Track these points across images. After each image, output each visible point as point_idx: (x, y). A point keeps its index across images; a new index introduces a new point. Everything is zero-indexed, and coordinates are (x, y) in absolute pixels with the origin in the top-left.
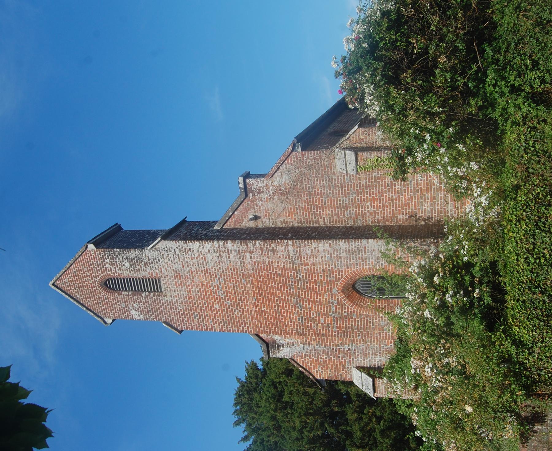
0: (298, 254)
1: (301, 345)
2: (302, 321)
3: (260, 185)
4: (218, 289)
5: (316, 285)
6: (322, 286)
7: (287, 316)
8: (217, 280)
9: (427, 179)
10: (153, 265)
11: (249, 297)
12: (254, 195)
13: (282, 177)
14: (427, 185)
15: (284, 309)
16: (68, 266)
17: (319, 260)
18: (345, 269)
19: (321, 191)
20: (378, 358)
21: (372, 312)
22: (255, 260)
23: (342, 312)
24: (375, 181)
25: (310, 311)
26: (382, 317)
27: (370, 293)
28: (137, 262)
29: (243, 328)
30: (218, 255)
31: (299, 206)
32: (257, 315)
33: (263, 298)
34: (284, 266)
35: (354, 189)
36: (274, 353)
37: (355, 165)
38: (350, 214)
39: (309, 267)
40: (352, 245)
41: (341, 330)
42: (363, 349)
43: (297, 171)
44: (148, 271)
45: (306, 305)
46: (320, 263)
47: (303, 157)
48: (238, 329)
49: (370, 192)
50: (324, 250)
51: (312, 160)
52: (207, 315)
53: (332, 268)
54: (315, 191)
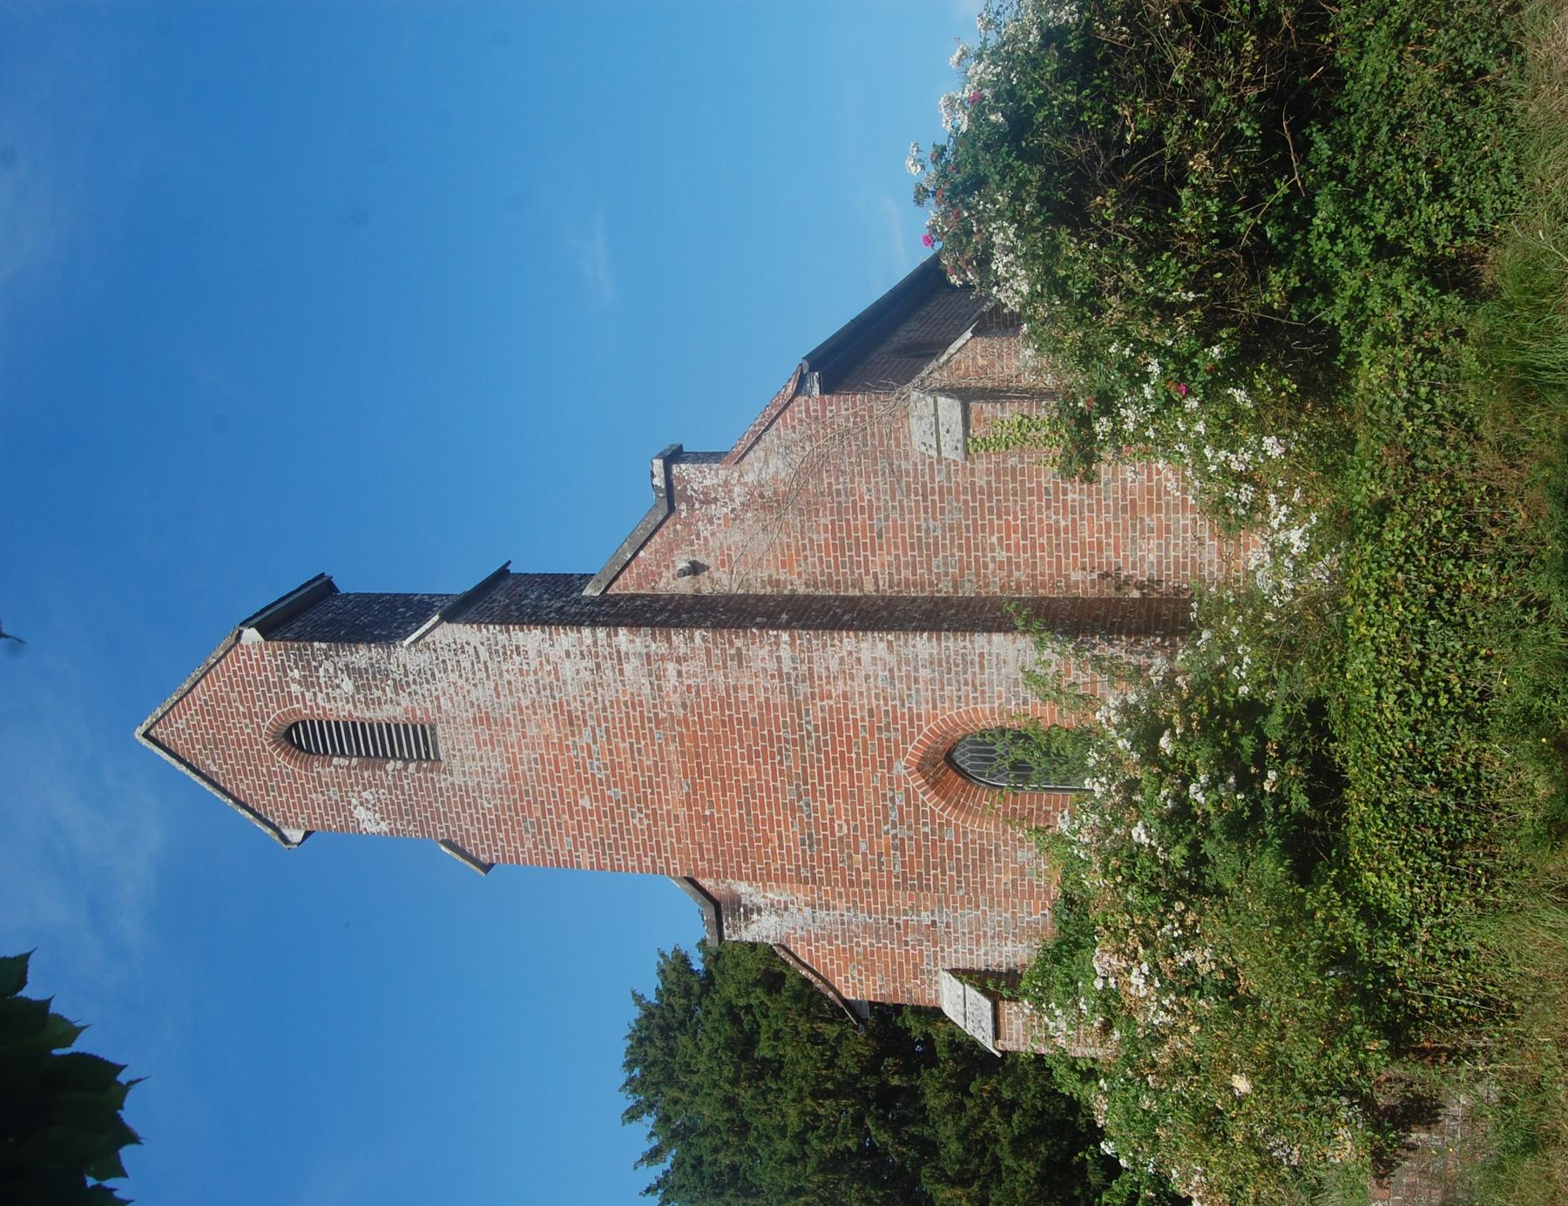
0: (805, 667)
1: (807, 911)
2: (811, 846)
3: (707, 482)
4: (590, 757)
5: (850, 752)
6: (865, 753)
7: (772, 831)
8: (587, 732)
9: (1150, 479)
10: (418, 688)
11: (672, 778)
12: (691, 508)
13: (766, 462)
14: (1150, 492)
15: (763, 813)
16: (186, 687)
17: (858, 685)
18: (928, 712)
19: (870, 501)
20: (1009, 948)
21: (996, 825)
22: (690, 682)
23: (917, 822)
24: (1014, 480)
25: (832, 820)
26: (1020, 840)
27: (991, 775)
28: (374, 679)
29: (653, 862)
30: (591, 664)
31: (811, 540)
32: (692, 828)
33: (708, 782)
34: (767, 699)
35: (958, 500)
36: (736, 929)
37: (960, 437)
38: (946, 564)
39: (832, 702)
40: (947, 648)
41: (912, 872)
42: (970, 924)
43: (808, 448)
44: (404, 704)
45: (823, 803)
46: (861, 693)
47: (824, 412)
48: (640, 863)
49: (999, 509)
50: (874, 659)
51: (848, 420)
52: (559, 825)
53: (894, 707)
54: (854, 502)
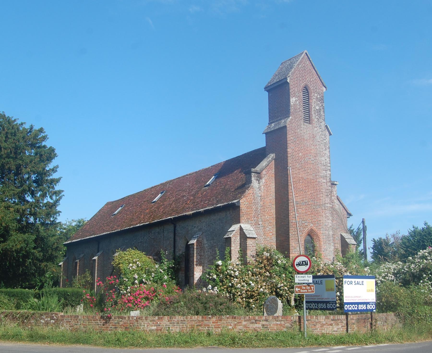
8: (313, 159)
30: (325, 164)
36: (254, 176)
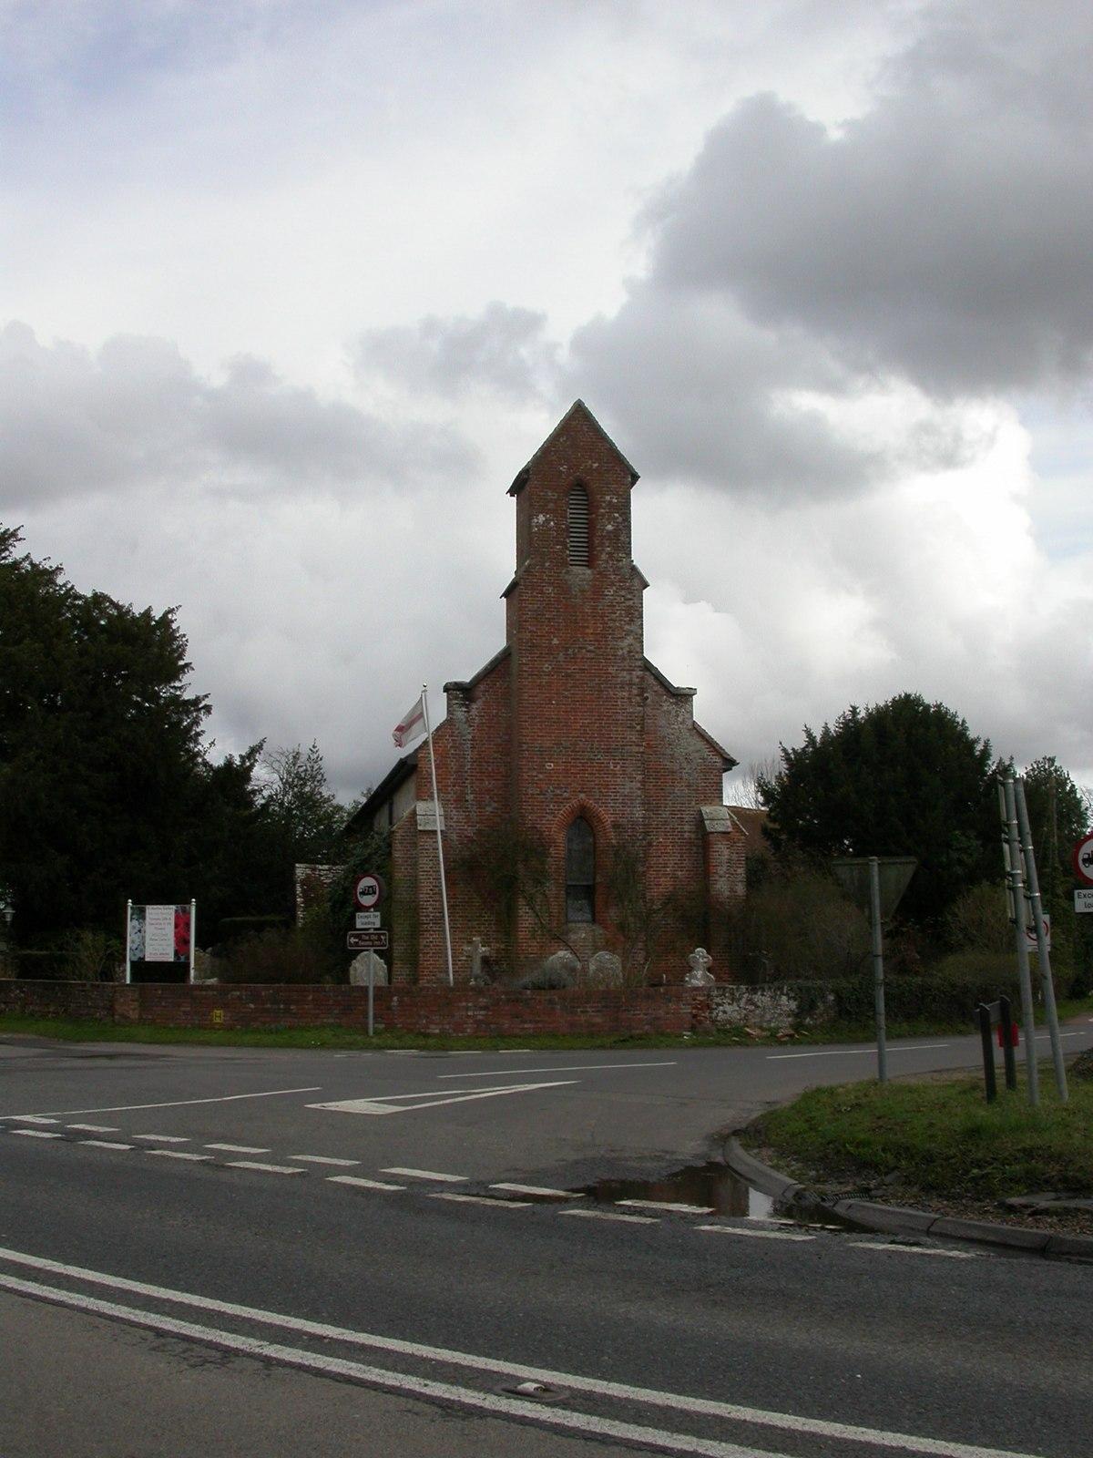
8: (592, 648)
23: (555, 802)
